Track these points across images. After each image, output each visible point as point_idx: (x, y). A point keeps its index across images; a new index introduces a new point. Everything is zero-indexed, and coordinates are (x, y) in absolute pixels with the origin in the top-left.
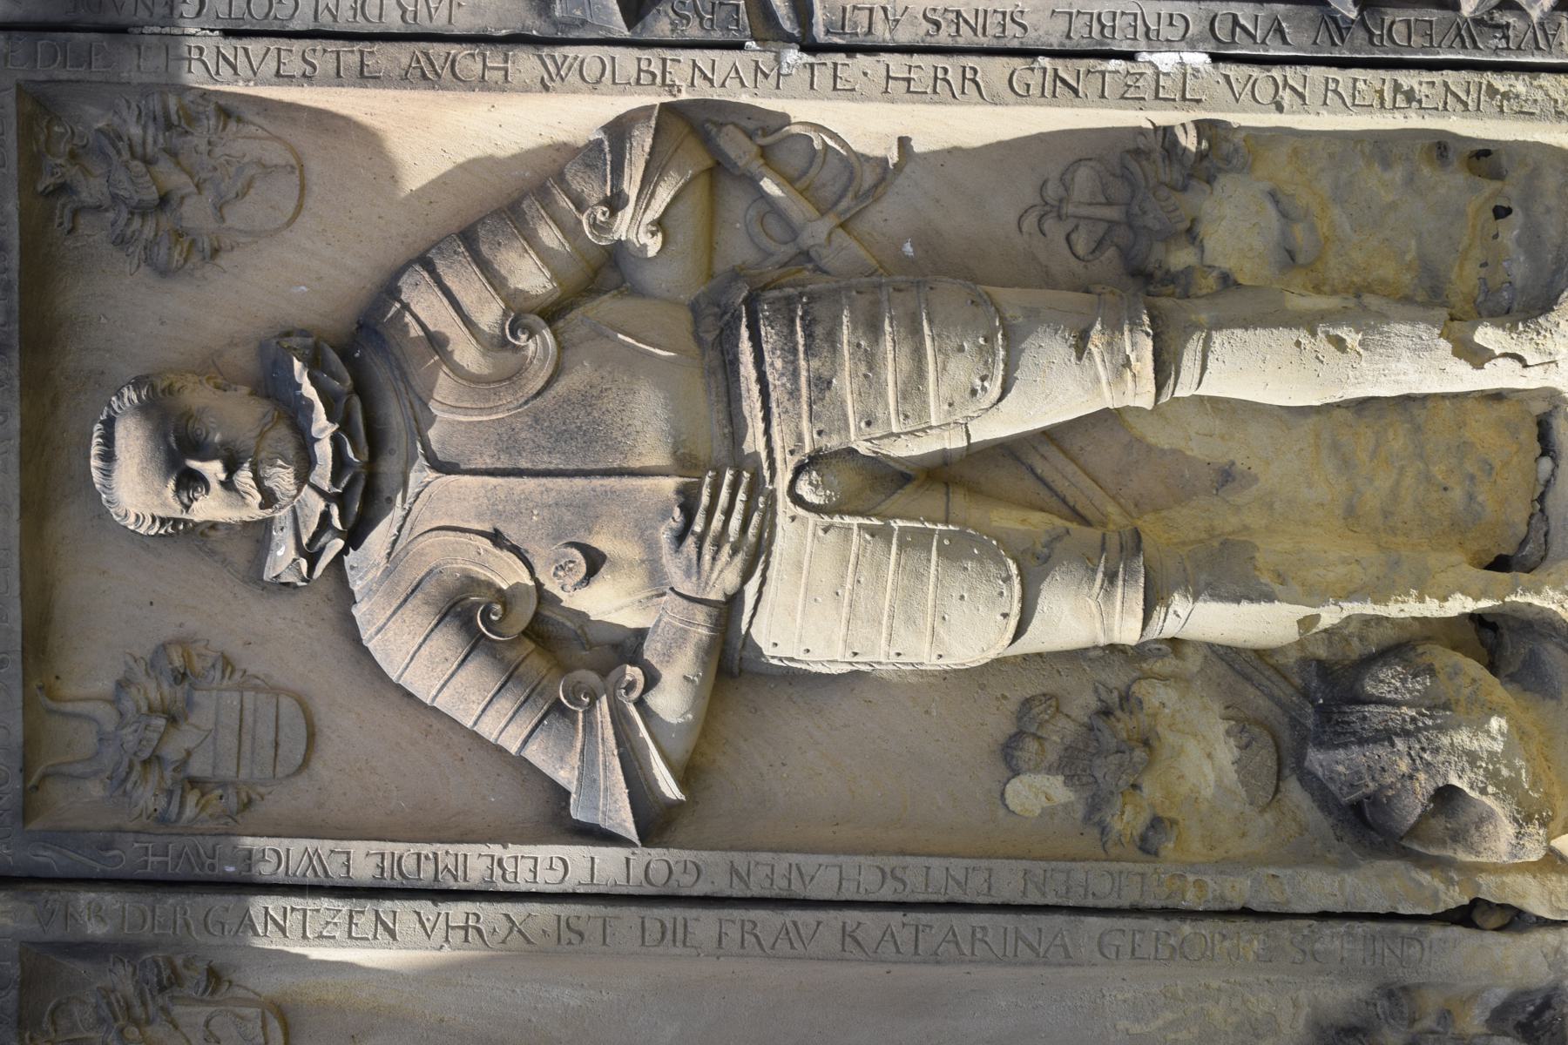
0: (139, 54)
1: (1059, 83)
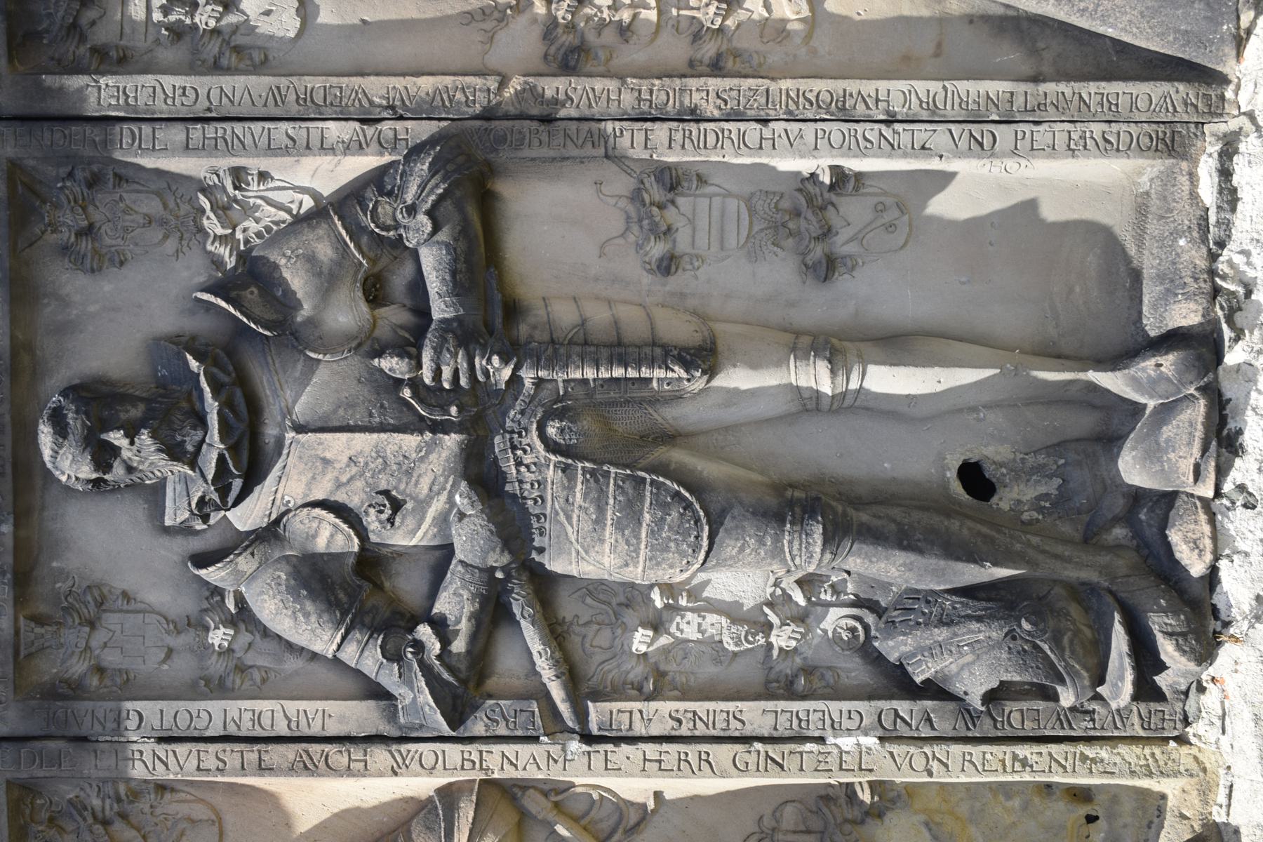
0: (96, 756)
1: (769, 761)
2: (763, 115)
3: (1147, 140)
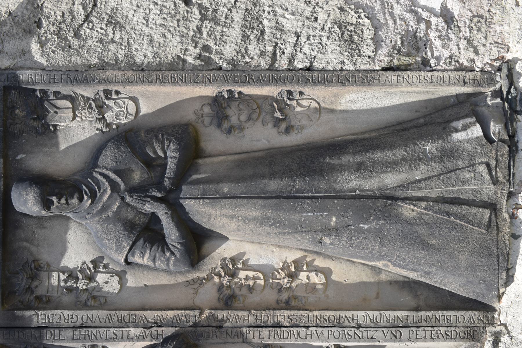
2: (306, 325)
3: (463, 334)
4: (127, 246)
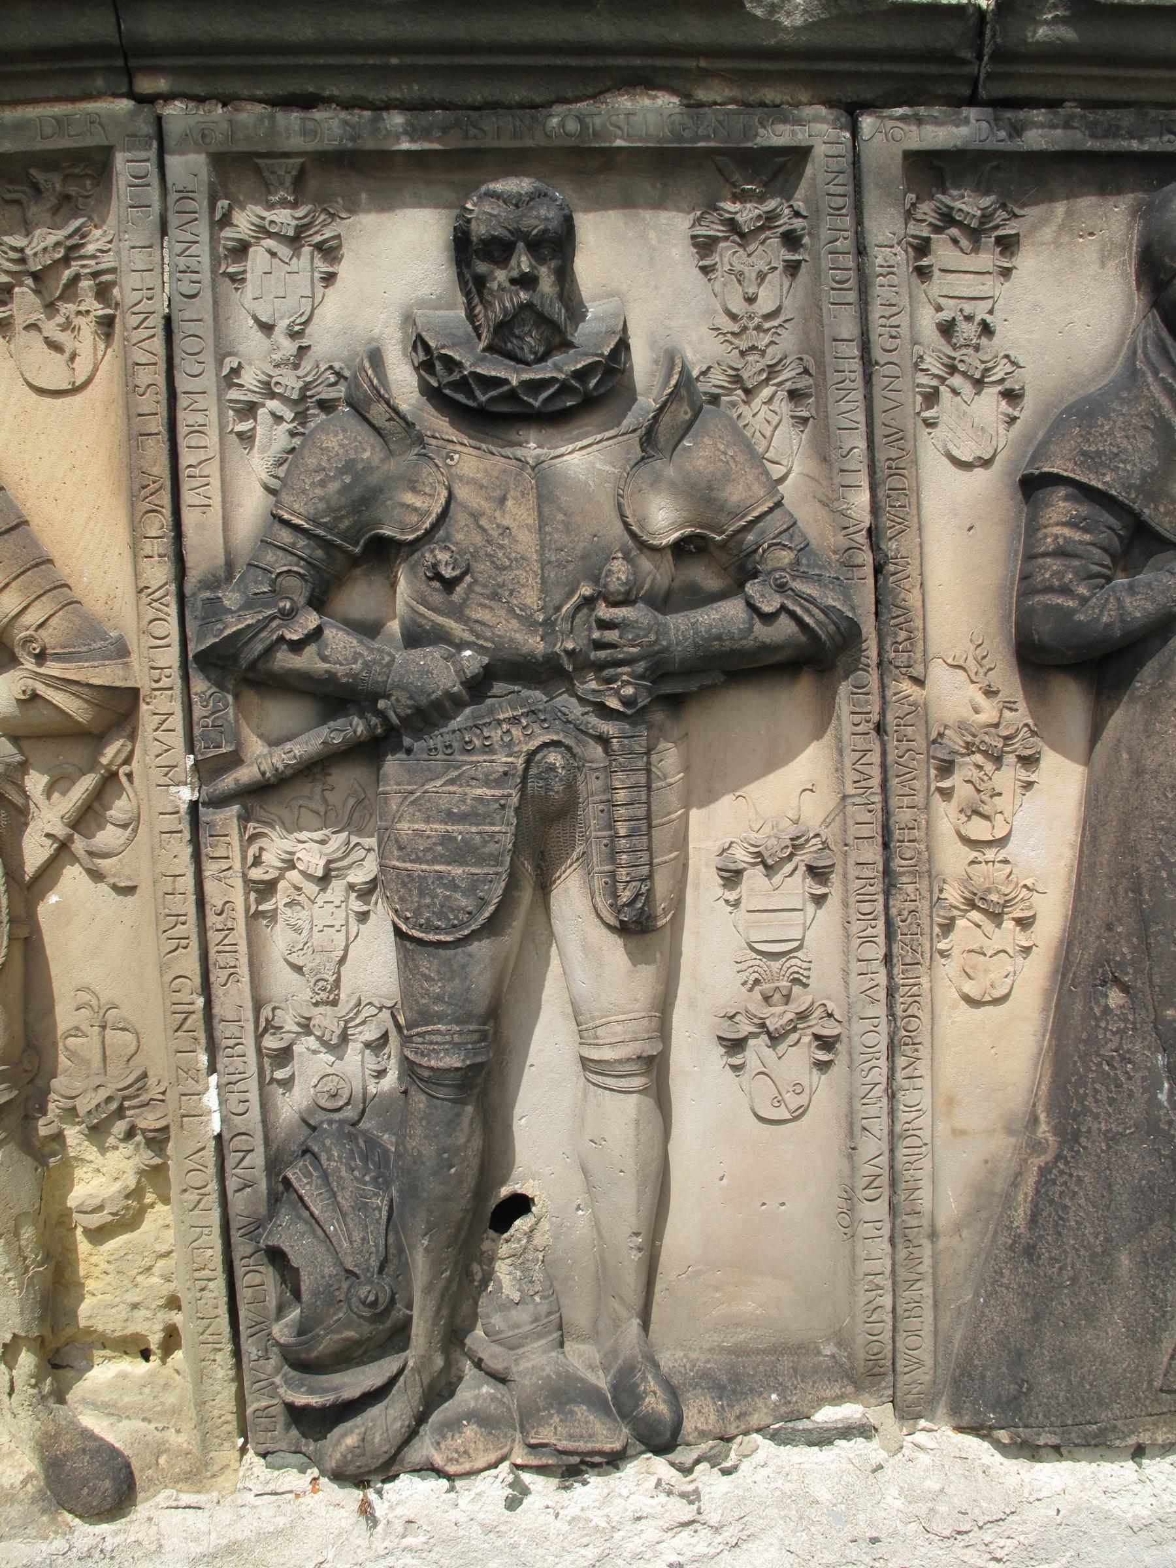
3: (875, 1350)
4: (1104, 483)
